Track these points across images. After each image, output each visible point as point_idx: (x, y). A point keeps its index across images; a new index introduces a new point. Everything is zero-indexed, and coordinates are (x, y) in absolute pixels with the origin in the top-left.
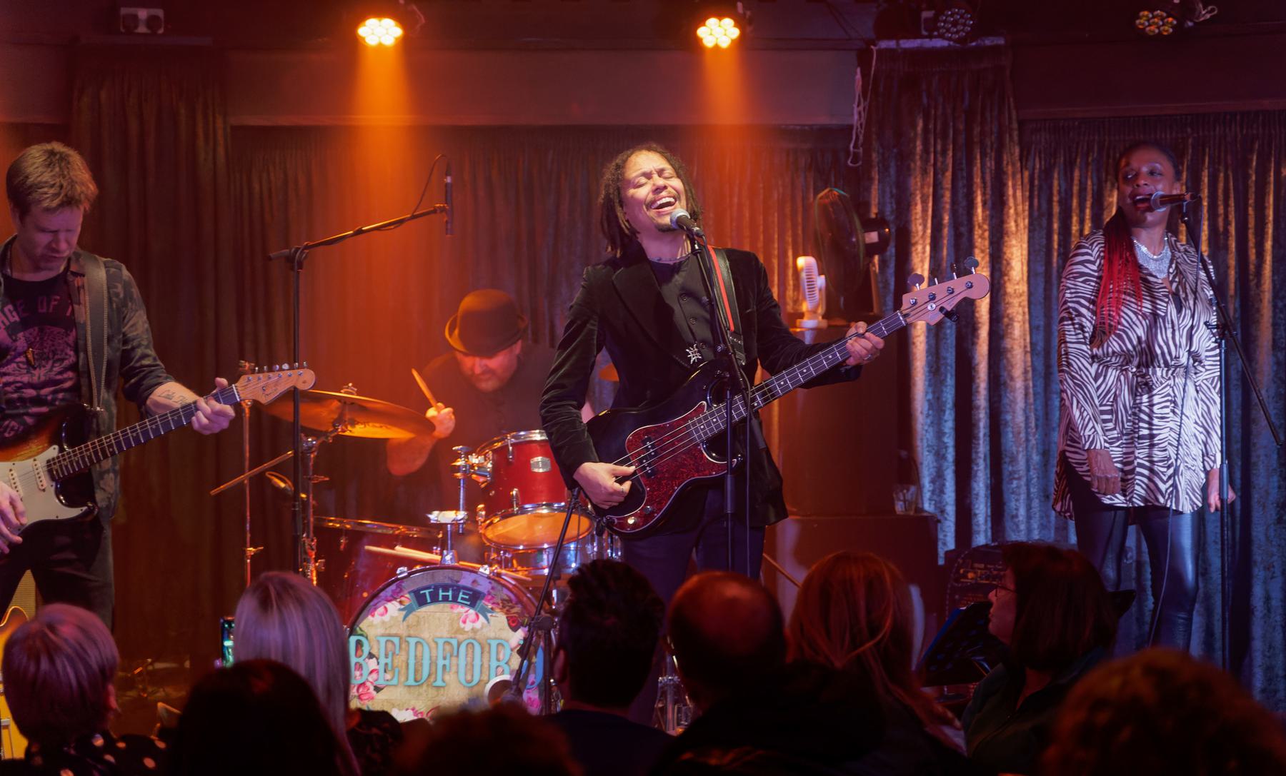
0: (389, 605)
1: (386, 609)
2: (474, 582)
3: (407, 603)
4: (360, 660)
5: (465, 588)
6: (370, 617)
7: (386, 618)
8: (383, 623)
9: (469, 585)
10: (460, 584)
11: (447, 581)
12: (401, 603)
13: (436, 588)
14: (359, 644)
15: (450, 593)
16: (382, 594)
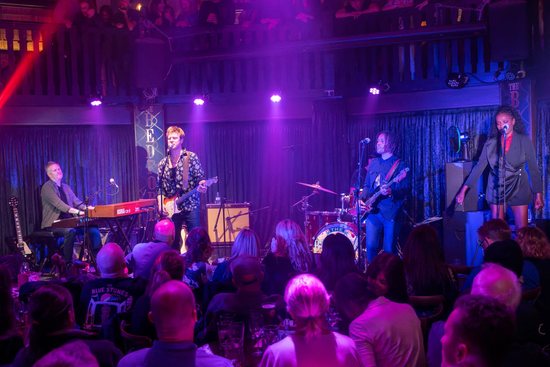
0: (323, 232)
1: (323, 233)
2: (343, 226)
3: (328, 232)
4: (317, 245)
5: (341, 228)
6: (319, 236)
7: (323, 235)
8: (322, 236)
9: (342, 227)
10: (340, 227)
11: (337, 226)
12: (326, 232)
13: (334, 228)
14: (317, 242)
15: (338, 229)
16: (322, 230)
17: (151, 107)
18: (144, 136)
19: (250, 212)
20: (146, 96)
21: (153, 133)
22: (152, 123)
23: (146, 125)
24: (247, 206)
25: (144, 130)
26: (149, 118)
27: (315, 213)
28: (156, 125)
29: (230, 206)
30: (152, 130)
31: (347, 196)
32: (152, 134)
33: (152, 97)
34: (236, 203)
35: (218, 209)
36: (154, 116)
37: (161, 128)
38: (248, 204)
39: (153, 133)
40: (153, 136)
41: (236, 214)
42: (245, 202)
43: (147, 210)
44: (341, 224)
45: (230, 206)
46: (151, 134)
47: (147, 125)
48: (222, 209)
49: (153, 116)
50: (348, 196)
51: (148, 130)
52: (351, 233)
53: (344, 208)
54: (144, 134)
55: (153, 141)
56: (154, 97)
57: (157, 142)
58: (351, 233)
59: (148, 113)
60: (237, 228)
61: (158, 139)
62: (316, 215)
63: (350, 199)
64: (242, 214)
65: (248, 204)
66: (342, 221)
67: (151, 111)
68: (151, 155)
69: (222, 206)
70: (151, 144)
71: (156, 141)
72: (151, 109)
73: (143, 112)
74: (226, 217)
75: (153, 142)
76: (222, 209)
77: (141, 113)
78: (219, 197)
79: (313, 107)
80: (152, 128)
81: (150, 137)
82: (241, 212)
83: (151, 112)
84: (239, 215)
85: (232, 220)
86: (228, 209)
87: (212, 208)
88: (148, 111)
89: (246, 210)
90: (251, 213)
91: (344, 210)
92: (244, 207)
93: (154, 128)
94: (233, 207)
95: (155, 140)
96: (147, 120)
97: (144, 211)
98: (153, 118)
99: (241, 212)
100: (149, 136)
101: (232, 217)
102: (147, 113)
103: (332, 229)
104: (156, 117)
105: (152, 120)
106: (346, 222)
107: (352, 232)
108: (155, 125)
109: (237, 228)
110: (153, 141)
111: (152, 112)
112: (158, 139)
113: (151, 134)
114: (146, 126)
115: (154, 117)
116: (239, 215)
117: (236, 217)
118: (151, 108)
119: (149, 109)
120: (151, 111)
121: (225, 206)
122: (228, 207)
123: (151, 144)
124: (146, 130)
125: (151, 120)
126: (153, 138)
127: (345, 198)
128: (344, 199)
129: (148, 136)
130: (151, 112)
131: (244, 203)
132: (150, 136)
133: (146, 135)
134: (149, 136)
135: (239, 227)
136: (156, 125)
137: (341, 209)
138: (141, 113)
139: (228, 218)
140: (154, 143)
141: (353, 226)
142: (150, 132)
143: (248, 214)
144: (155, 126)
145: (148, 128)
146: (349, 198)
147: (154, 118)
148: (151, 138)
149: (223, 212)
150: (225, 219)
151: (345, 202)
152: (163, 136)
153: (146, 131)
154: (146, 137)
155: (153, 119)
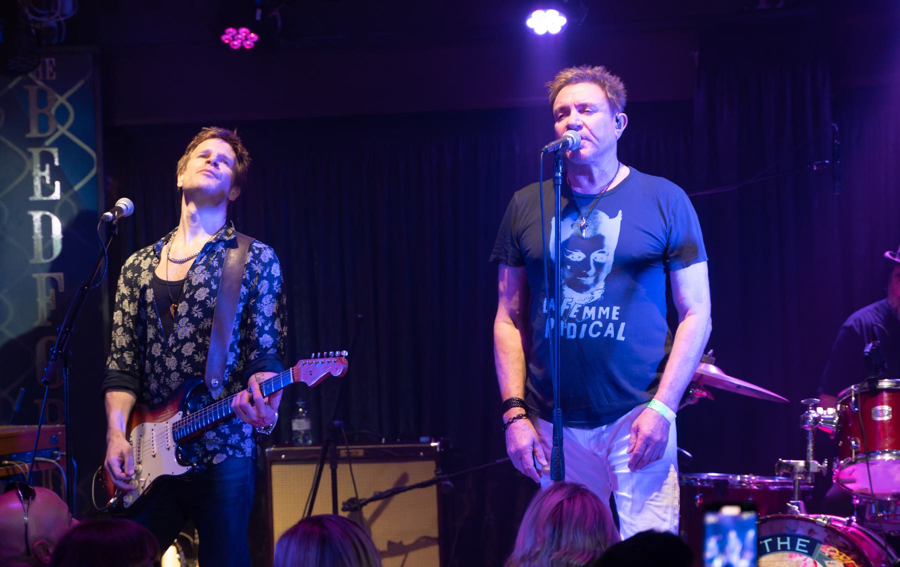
17: (47, 60)
18: (23, 176)
19: (440, 479)
20: (31, 17)
21: (57, 163)
22: (53, 123)
23: (28, 131)
24: (430, 454)
25: (24, 156)
26: (43, 101)
27: (702, 481)
28: (70, 130)
29: (361, 453)
30: (55, 152)
31: (825, 409)
32: (53, 167)
33: (53, 23)
34: (385, 444)
35: (312, 469)
36: (62, 94)
37: (92, 148)
38: (433, 444)
39: (57, 163)
40: (56, 174)
41: (386, 485)
42: (423, 439)
43: (24, 467)
44: (801, 523)
45: (361, 453)
46: (47, 166)
47: (34, 133)
48: (327, 469)
49: (57, 96)
50: (831, 411)
51: (36, 152)
52: (842, 557)
53: (815, 459)
54: (21, 169)
55: (56, 195)
56: (62, 19)
57: (75, 196)
58: (842, 557)
59: (39, 83)
60: (390, 544)
61: (77, 187)
62: (702, 490)
63: (839, 421)
64: (408, 484)
65: (433, 444)
66: (809, 512)
67: (51, 75)
68: (49, 250)
69: (328, 455)
70: (50, 206)
71: (70, 193)
72: (49, 69)
73: (19, 78)
74: (342, 498)
75: (55, 202)
76: (327, 469)
77: (11, 85)
78: (307, 417)
79: (696, 54)
80: (52, 145)
81: (43, 178)
82: (404, 477)
83: (48, 77)
84: (398, 489)
85: (368, 511)
86: (356, 467)
87: (287, 462)
88: (37, 75)
89: (422, 470)
90: (445, 479)
91: (815, 465)
92: (417, 458)
93: (61, 143)
94: (371, 457)
95: (63, 190)
96: (34, 112)
97: (11, 473)
98: (57, 104)
99: (404, 477)
100: (41, 175)
101: (370, 495)
102: (32, 83)
103: (766, 542)
104: (69, 100)
105: (53, 111)
106: (823, 516)
107: (848, 554)
108: (63, 130)
109: (390, 544)
110: (56, 195)
111: (54, 78)
112: (77, 187)
113: (47, 166)
114: (28, 136)
115: (62, 100)
116: (398, 489)
117: (385, 497)
118: (51, 62)
119: (40, 69)
120: (51, 75)
121: (343, 453)
122: (351, 460)
123: (50, 206)
124: (30, 150)
125: (50, 110)
126: (57, 184)
127: (820, 417)
128: (816, 420)
129: (38, 174)
130: (48, 77)
131: (419, 442)
132: (46, 173)
133: (31, 172)
134: (41, 175)
135: (397, 541)
136: (70, 130)
137: (802, 463)
138: (11, 85)
139: (352, 501)
140: (59, 205)
141: (852, 532)
142: (46, 158)
143: (433, 489)
144: (63, 137)
145: (39, 142)
146: (837, 419)
147: (62, 108)
148: (48, 181)
149: (330, 477)
150: (340, 506)
151: (820, 434)
152: (96, 176)
153: (30, 155)
154: (30, 179)
155: (57, 111)
